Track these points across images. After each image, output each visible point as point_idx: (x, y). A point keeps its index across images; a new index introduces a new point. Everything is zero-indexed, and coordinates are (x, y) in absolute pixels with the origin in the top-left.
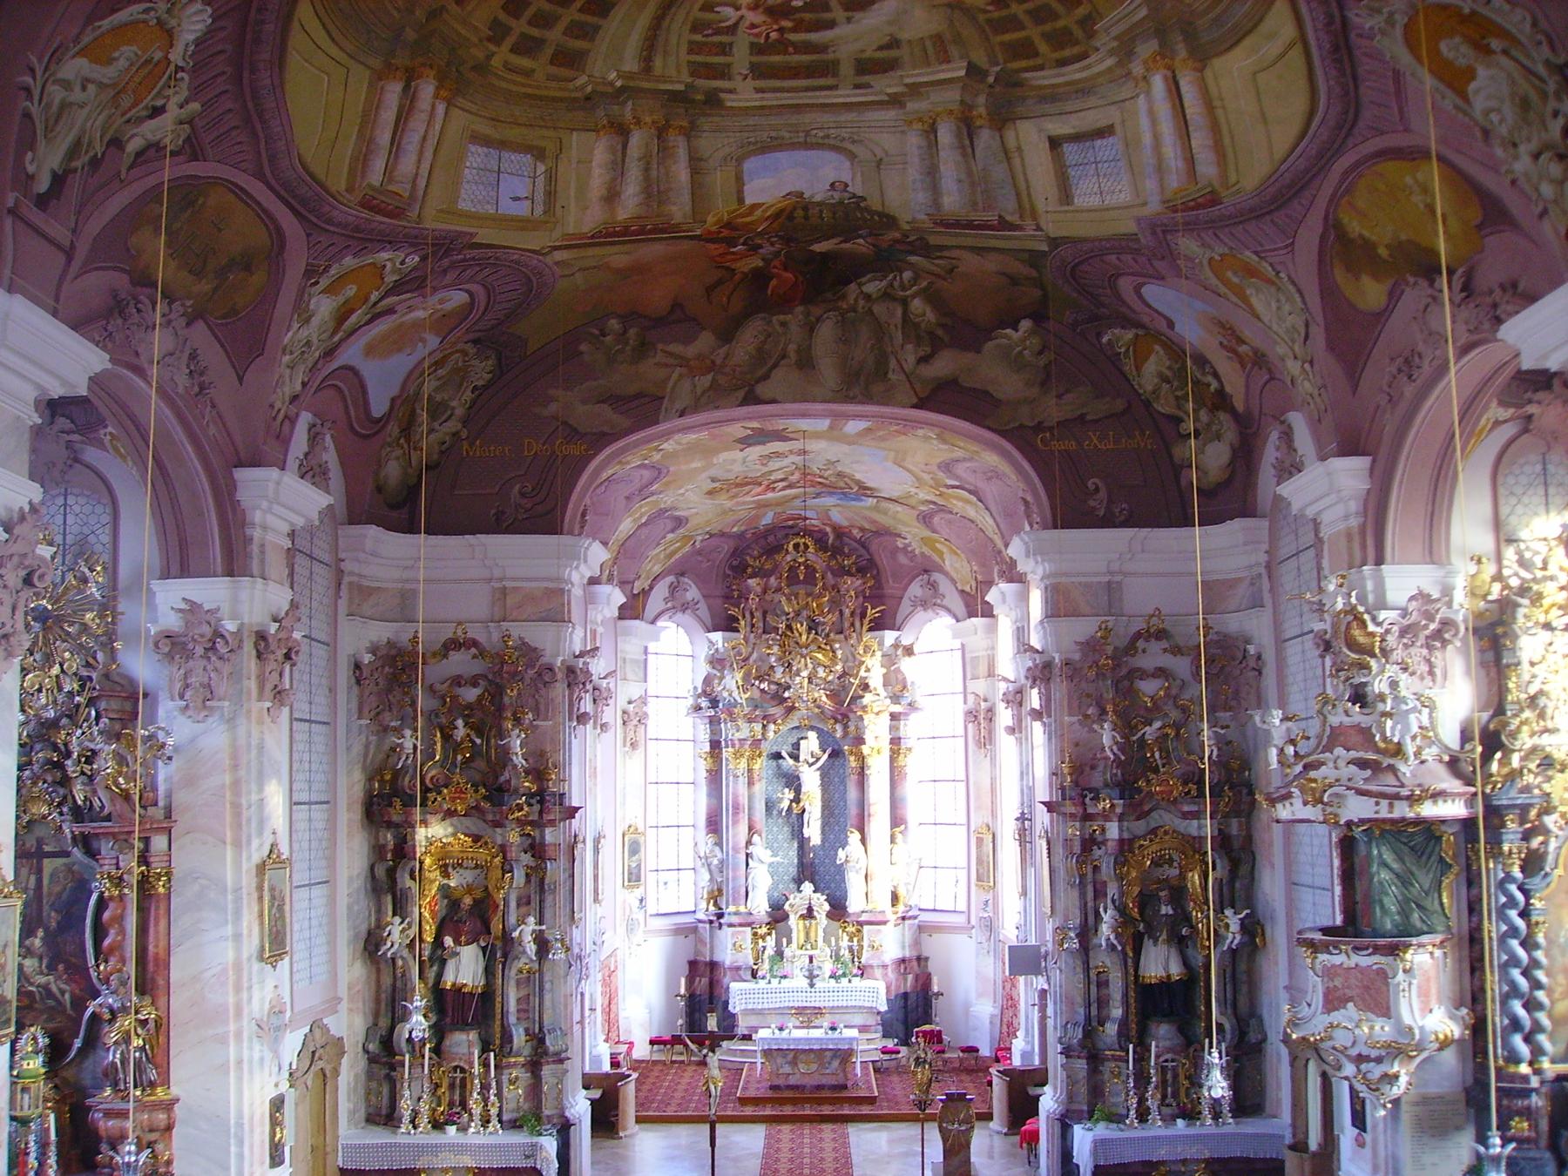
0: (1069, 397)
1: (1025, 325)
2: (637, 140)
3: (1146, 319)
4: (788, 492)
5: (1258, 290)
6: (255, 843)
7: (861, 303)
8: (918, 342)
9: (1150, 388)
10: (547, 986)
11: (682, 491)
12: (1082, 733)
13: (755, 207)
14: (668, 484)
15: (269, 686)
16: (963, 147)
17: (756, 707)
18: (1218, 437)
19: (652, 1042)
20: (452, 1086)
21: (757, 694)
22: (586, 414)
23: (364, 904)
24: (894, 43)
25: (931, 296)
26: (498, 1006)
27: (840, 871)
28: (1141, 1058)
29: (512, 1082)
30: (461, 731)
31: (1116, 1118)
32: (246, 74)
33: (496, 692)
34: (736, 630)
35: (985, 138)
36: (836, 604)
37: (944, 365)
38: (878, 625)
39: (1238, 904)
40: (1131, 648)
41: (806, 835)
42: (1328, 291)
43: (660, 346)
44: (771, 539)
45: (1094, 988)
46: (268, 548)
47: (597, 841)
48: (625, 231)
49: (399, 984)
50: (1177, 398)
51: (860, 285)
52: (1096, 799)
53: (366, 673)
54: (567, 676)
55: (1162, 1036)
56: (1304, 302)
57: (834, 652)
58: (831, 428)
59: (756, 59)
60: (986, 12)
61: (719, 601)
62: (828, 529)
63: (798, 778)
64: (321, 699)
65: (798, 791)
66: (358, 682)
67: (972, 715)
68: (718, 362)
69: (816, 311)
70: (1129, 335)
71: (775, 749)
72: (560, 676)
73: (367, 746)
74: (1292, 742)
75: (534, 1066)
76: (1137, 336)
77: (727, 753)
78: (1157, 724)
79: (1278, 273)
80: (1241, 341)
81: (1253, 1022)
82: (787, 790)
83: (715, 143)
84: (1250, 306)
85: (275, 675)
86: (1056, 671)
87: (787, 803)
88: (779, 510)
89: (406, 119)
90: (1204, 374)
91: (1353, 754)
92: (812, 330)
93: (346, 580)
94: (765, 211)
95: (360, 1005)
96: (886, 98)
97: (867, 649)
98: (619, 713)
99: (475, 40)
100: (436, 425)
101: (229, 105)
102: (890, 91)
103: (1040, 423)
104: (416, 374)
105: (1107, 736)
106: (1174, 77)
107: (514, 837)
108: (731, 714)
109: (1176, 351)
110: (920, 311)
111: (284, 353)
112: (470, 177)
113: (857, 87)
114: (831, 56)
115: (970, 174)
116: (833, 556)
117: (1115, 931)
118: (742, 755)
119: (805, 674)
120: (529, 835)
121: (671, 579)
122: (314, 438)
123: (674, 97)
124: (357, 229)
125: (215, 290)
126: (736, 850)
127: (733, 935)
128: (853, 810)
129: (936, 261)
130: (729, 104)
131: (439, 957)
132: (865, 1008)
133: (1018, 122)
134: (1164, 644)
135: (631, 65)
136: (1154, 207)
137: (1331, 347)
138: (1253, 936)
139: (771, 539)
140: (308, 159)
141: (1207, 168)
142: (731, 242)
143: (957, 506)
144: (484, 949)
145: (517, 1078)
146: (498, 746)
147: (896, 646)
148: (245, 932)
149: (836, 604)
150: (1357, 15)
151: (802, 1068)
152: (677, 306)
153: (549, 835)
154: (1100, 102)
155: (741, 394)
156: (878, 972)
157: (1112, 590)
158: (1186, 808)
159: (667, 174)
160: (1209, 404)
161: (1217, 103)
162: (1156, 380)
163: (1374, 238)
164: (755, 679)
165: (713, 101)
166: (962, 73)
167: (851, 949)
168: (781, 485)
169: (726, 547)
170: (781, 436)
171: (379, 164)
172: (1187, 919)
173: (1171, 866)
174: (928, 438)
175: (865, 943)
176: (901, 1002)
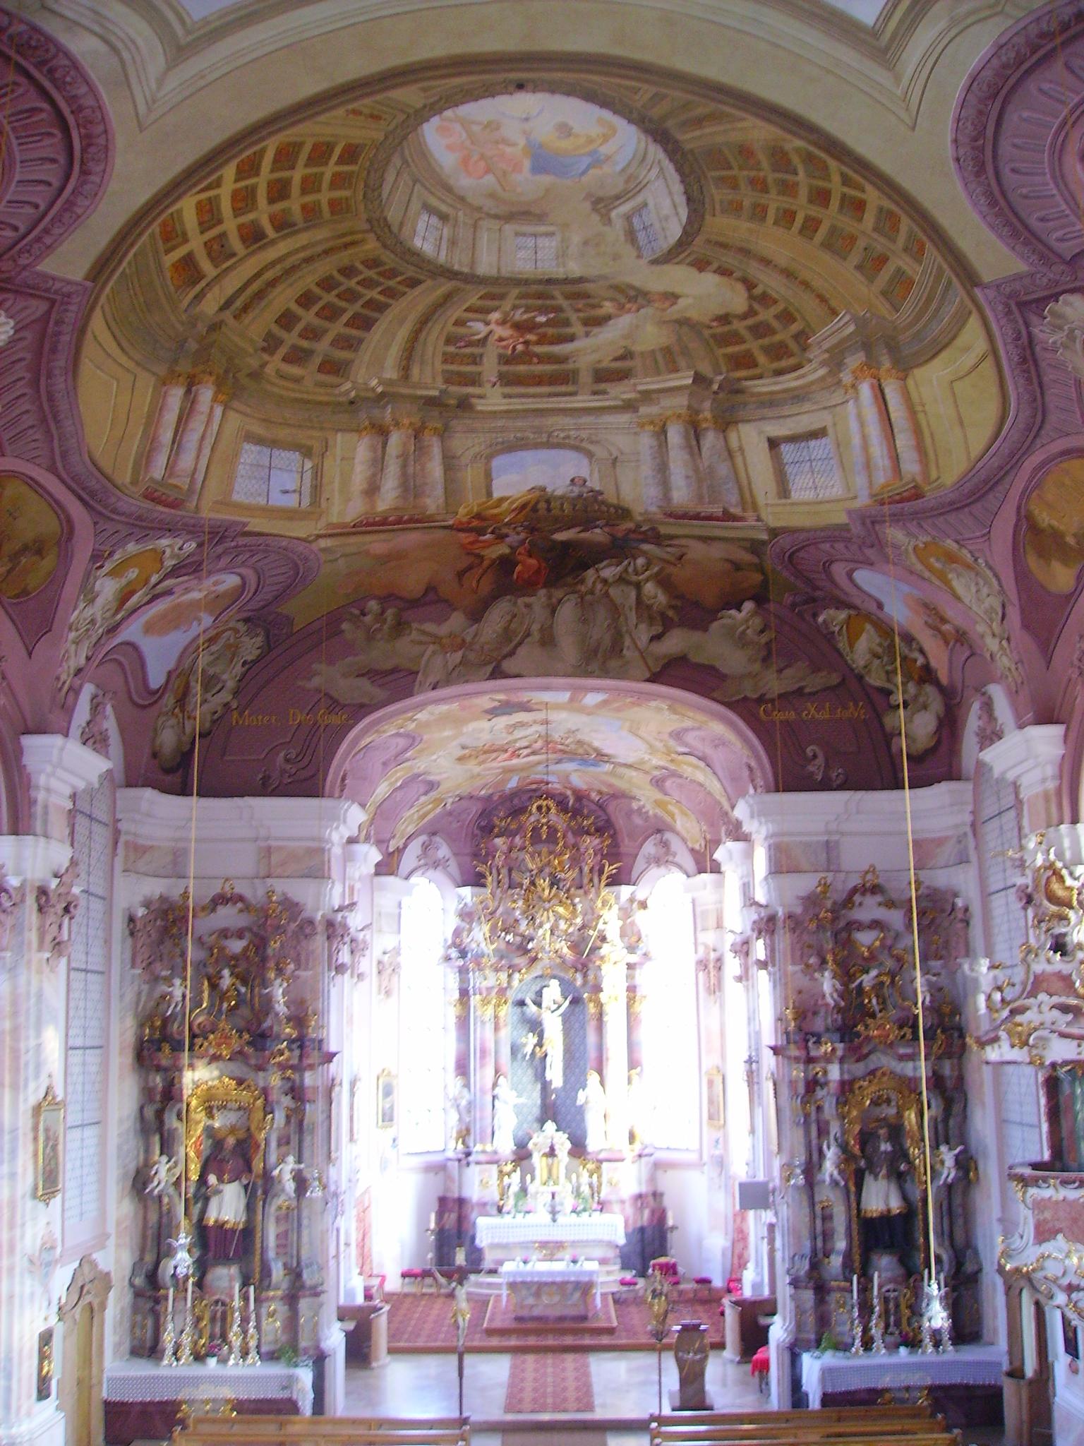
0: (788, 672)
1: (748, 606)
2: (395, 440)
3: (858, 602)
4: (532, 758)
5: (958, 575)
6: (32, 1085)
7: (599, 586)
8: (651, 621)
9: (862, 663)
10: (305, 1222)
11: (434, 757)
12: (804, 982)
13: (502, 500)
14: (422, 751)
15: (49, 938)
16: (690, 447)
17: (502, 958)
18: (925, 707)
19: (404, 1275)
20: (213, 1319)
21: (503, 946)
22: (348, 688)
23: (133, 1144)
24: (627, 355)
25: (664, 582)
26: (258, 1241)
27: (581, 1111)
28: (865, 1289)
29: (271, 1315)
30: (227, 980)
31: (843, 1347)
32: (43, 379)
33: (260, 944)
34: (484, 886)
35: (710, 440)
36: (576, 861)
37: (675, 642)
38: (615, 881)
39: (952, 1141)
40: (848, 902)
41: (548, 1078)
42: (1022, 576)
43: (414, 625)
44: (516, 801)
45: (819, 1222)
46: (51, 810)
47: (353, 1084)
48: (384, 522)
49: (165, 1220)
50: (887, 673)
51: (597, 570)
52: (818, 1042)
53: (139, 926)
54: (327, 930)
55: (884, 1267)
56: (1000, 585)
57: (574, 905)
58: (572, 700)
59: (505, 368)
60: (710, 327)
61: (468, 859)
62: (569, 793)
63: (540, 1024)
64: (97, 950)
65: (541, 1036)
66: (132, 934)
67: (702, 965)
68: (468, 639)
69: (558, 593)
70: (842, 615)
71: (519, 997)
72: (320, 928)
73: (139, 994)
74: (999, 989)
75: (292, 1299)
76: (849, 617)
77: (475, 1000)
78: (874, 973)
79: (976, 560)
80: (943, 620)
81: (969, 1252)
83: (467, 443)
84: (952, 588)
85: (55, 928)
86: (780, 924)
88: (524, 774)
89: (187, 420)
90: (911, 650)
91: (1056, 1000)
92: (553, 612)
93: (122, 839)
94: (512, 503)
95: (127, 1240)
96: (620, 403)
97: (604, 903)
98: (375, 963)
99: (251, 350)
100: (208, 696)
101: (27, 407)
102: (625, 396)
103: (763, 695)
104: (191, 650)
105: (828, 984)
106: (880, 385)
107: (275, 1080)
108: (478, 964)
109: (885, 629)
110: (652, 593)
111: (70, 629)
112: (243, 472)
113: (595, 393)
114: (570, 366)
115: (696, 470)
116: (573, 817)
117: (838, 1167)
118: (489, 1003)
119: (547, 926)
120: (289, 1079)
121: (423, 838)
122: (96, 708)
123: (430, 402)
124: (140, 518)
125: (9, 572)
126: (483, 1092)
128: (592, 1053)
129: (669, 549)
130: (479, 408)
131: (203, 1194)
133: (740, 425)
134: (879, 898)
135: (391, 373)
136: (863, 500)
137: (1026, 626)
138: (967, 1172)
139: (516, 801)
140: (97, 454)
141: (911, 466)
142: (481, 532)
143: (688, 771)
144: (246, 1187)
145: (275, 1311)
146: (261, 996)
147: (632, 900)
148: (20, 1170)
149: (576, 861)
151: (545, 1299)
152: (431, 589)
153: (309, 1079)
154: (815, 407)
155: (489, 669)
156: (616, 1207)
157: (830, 848)
158: (902, 1051)
159: (423, 469)
160: (916, 677)
161: (919, 408)
162: (868, 656)
163: (1062, 528)
164: (502, 930)
165: (464, 405)
166: (690, 381)
167: (591, 1186)
168: (525, 752)
169: (475, 809)
170: (525, 707)
171: (161, 460)
172: (905, 1156)
173: (889, 1105)
174: (659, 710)
175: (604, 1179)
176: (637, 1237)
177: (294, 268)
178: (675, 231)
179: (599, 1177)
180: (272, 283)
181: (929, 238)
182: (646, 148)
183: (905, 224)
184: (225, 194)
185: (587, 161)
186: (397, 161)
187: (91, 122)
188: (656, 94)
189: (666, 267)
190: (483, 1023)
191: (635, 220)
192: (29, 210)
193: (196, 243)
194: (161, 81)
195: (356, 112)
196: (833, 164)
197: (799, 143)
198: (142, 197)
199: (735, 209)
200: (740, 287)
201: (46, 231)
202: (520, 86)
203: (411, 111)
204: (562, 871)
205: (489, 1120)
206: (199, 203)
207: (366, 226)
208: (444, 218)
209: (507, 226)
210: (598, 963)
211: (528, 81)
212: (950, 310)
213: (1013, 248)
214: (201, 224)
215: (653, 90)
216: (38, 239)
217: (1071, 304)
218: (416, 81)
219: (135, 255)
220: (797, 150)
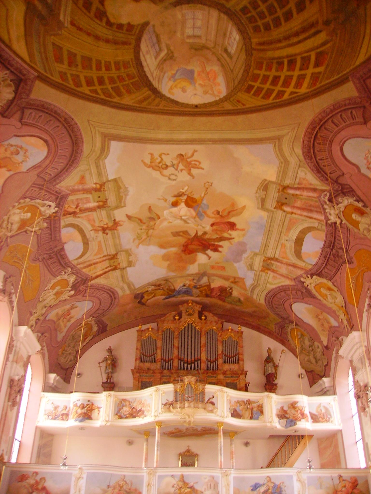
150: (6, 74)
177: (287, 38)
178: (143, 46)
180: (297, 34)
181: (62, 84)
182: (159, 85)
183: (72, 85)
184: (291, 89)
185: (177, 77)
186: (236, 83)
187: (310, 133)
188: (158, 106)
189: (142, 21)
191: (158, 49)
192: (344, 115)
193: (311, 70)
194: (288, 134)
195: (243, 105)
196: (103, 97)
197: (115, 100)
198: (315, 101)
199: (126, 65)
200: (112, 20)
201: (345, 105)
202: (196, 106)
203: (228, 101)
206: (300, 88)
207: (254, 53)
208: (226, 51)
209: (203, 41)
211: (194, 108)
212: (37, 58)
213: (40, 101)
214: (304, 79)
215: (159, 108)
216: (349, 104)
217: (10, 93)
218: (225, 110)
219: (330, 79)
220: (115, 97)
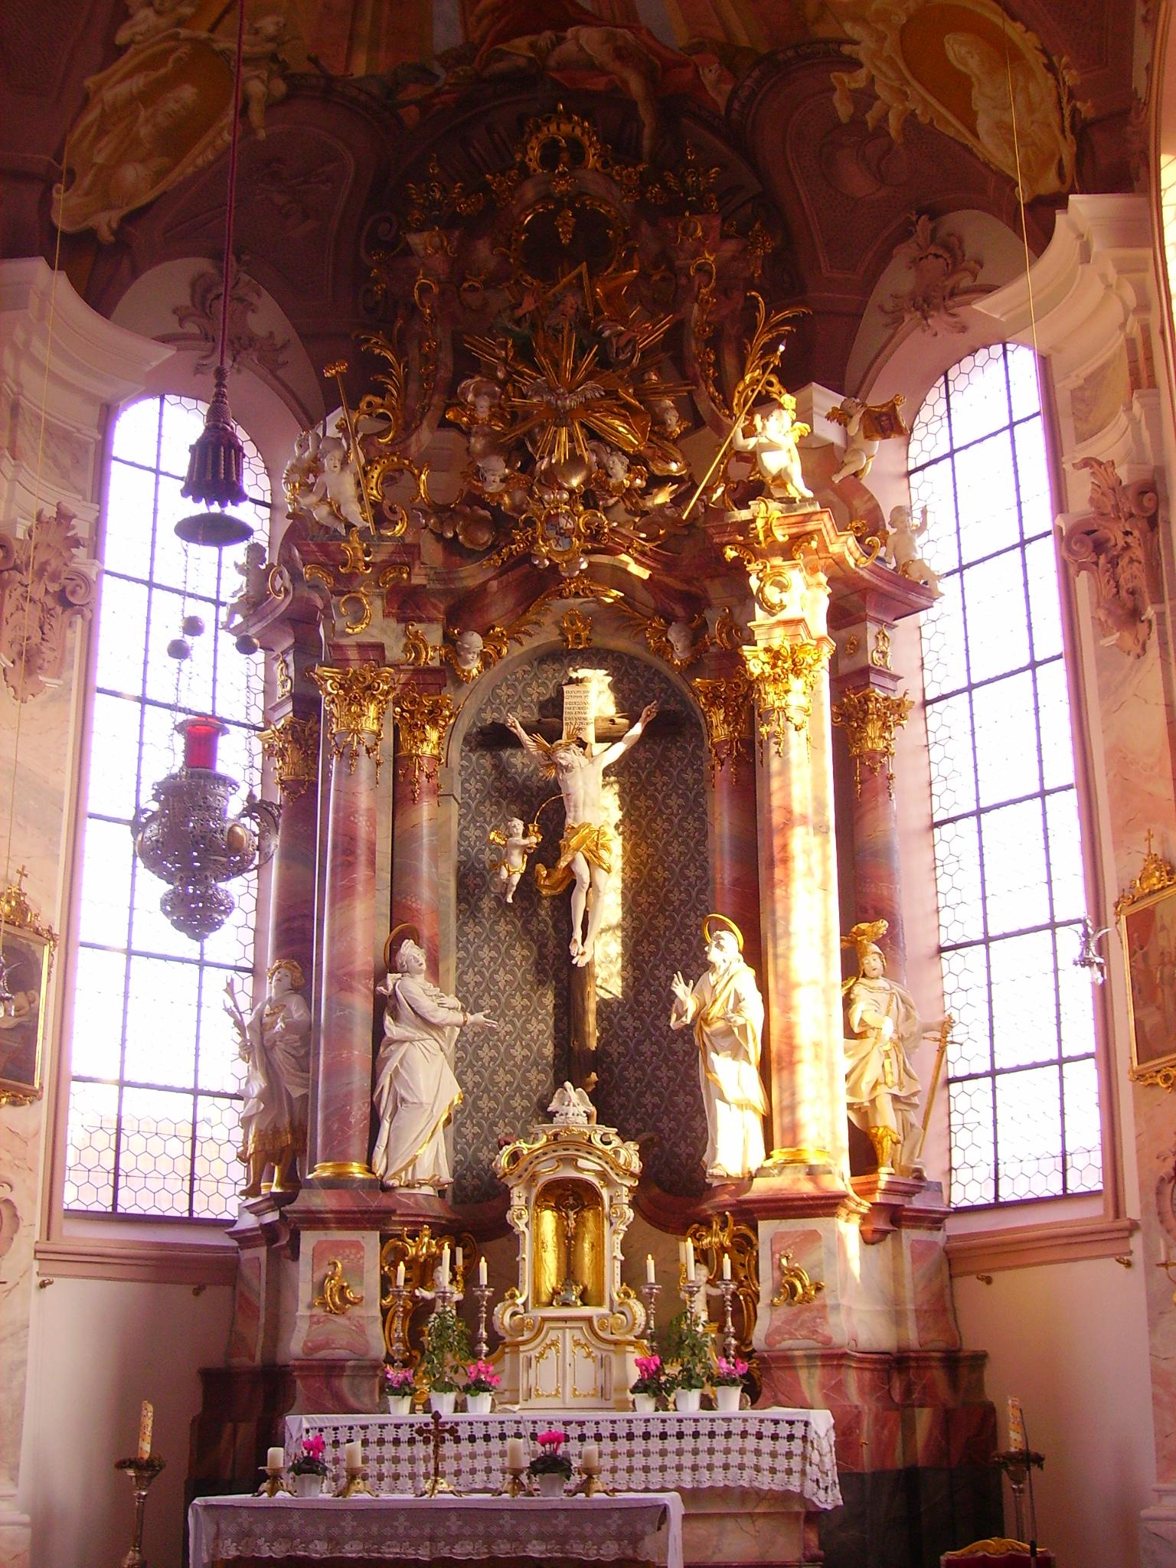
41: (580, 961)
62: (636, 85)
71: (489, 717)
82: (518, 825)
87: (518, 863)
119: (575, 482)
127: (318, 1255)
128: (724, 871)
132: (760, 1495)
156: (810, 1381)
167: (716, 1311)
175: (765, 1287)
179: (746, 1272)
190: (349, 756)
204: (623, 320)
205: (359, 1079)
210: (730, 553)
